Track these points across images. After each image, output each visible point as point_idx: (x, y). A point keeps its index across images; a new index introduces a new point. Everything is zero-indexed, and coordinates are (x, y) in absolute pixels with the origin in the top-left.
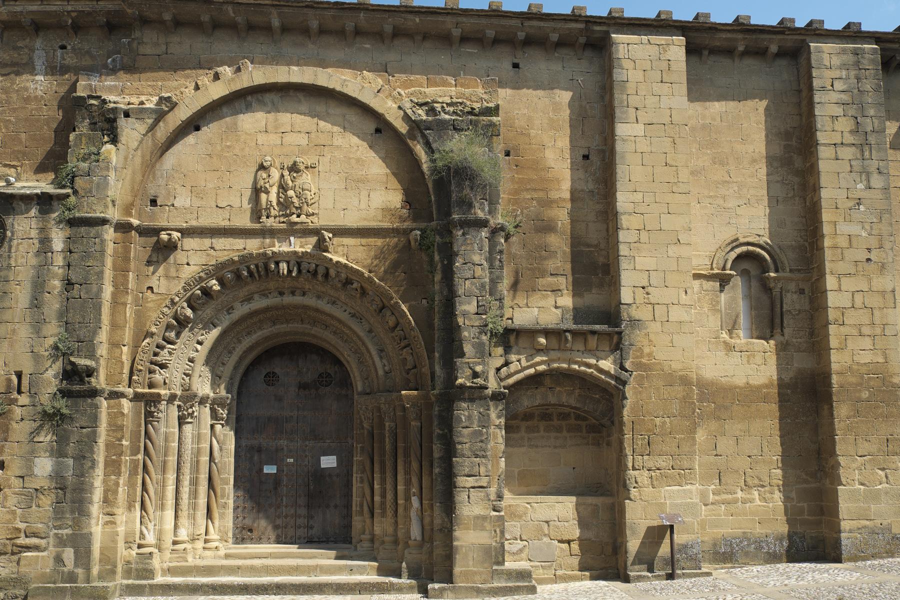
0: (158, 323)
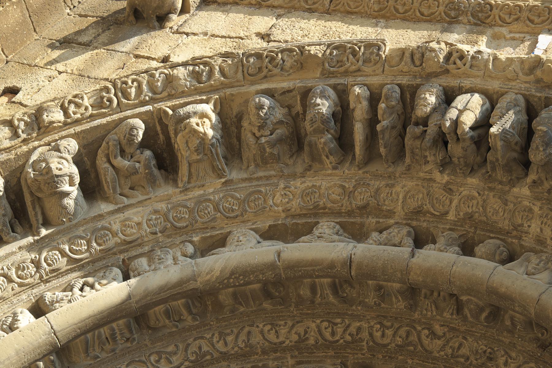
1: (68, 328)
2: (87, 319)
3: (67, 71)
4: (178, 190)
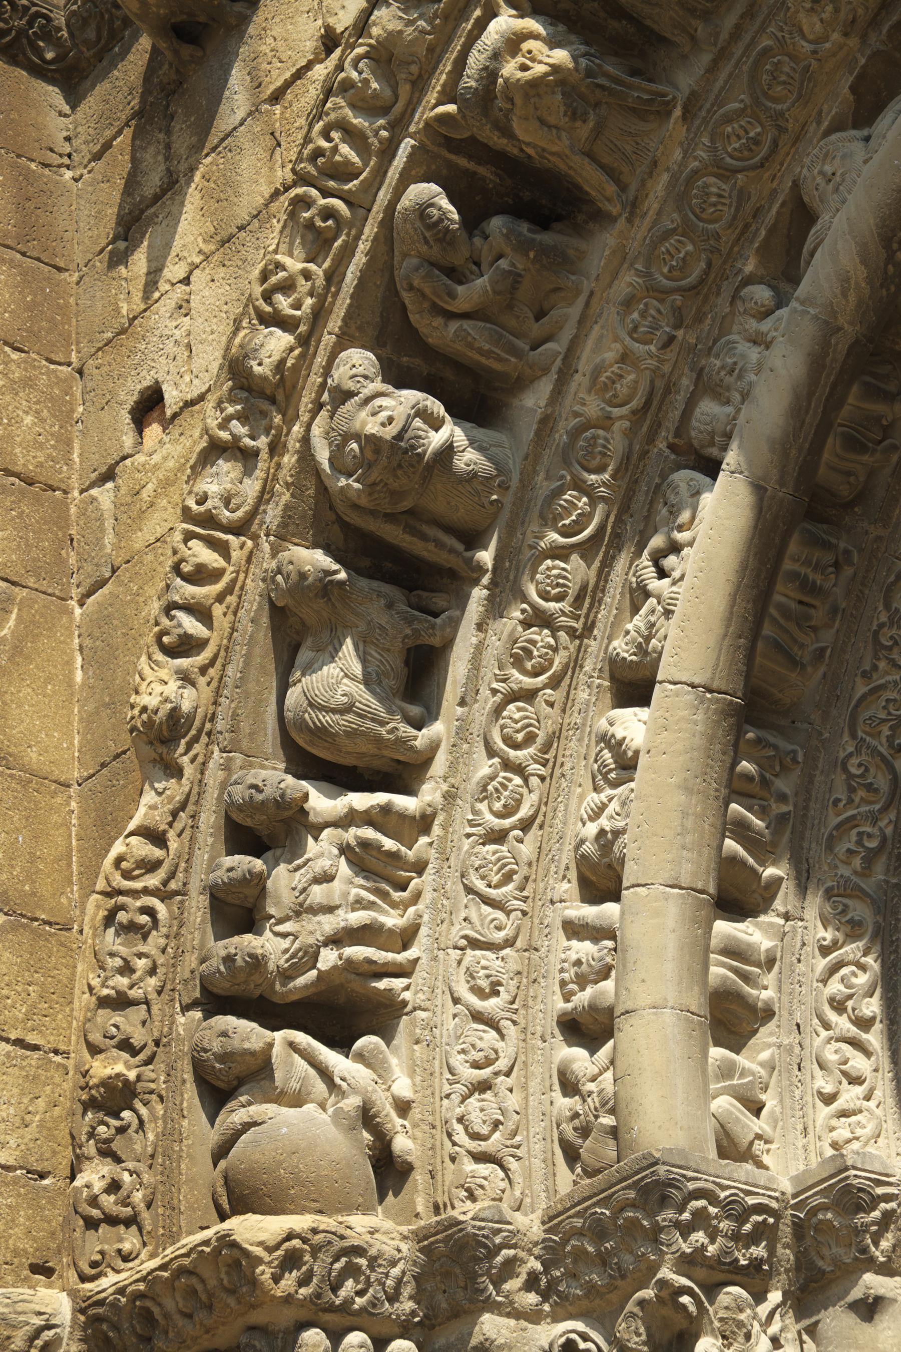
0: (190, 625)
1: (718, 659)
2: (732, 606)
3: (192, 263)
4: (621, 223)
